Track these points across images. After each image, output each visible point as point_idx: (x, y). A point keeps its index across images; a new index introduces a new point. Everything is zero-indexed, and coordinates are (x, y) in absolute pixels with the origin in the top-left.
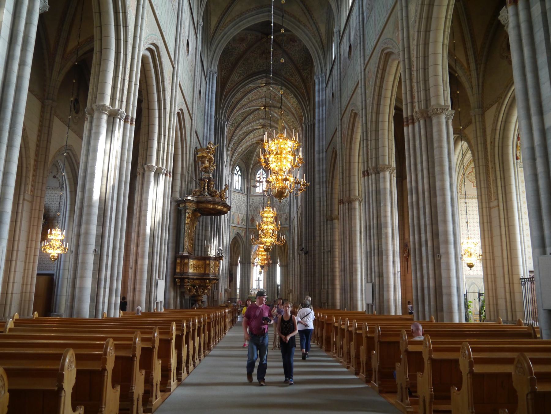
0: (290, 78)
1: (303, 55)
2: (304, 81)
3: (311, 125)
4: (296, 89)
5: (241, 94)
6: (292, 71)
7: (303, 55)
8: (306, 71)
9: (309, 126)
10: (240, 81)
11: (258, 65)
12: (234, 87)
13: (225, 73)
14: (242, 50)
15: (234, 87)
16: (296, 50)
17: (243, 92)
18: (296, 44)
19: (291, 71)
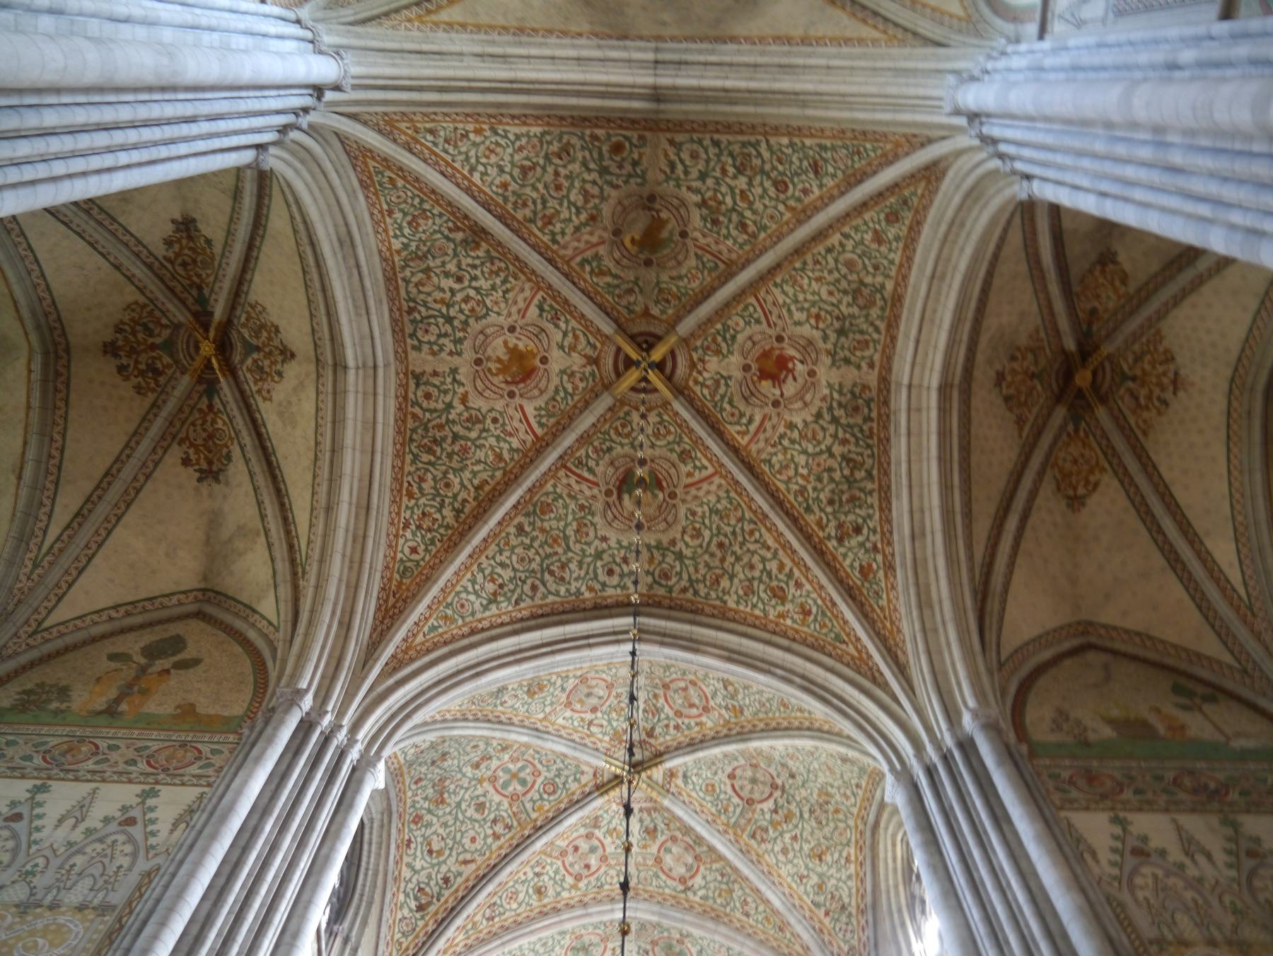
0: (772, 614)
1: (829, 450)
2: (851, 594)
3: (947, 758)
4: (815, 655)
5: (496, 837)
6: (781, 567)
7: (829, 450)
8: (855, 541)
9: (930, 772)
10: (492, 627)
11: (599, 555)
12: (453, 639)
13: (414, 550)
14: (515, 443)
15: (453, 639)
16: (791, 426)
17: (509, 827)
18: (790, 388)
19: (773, 566)
